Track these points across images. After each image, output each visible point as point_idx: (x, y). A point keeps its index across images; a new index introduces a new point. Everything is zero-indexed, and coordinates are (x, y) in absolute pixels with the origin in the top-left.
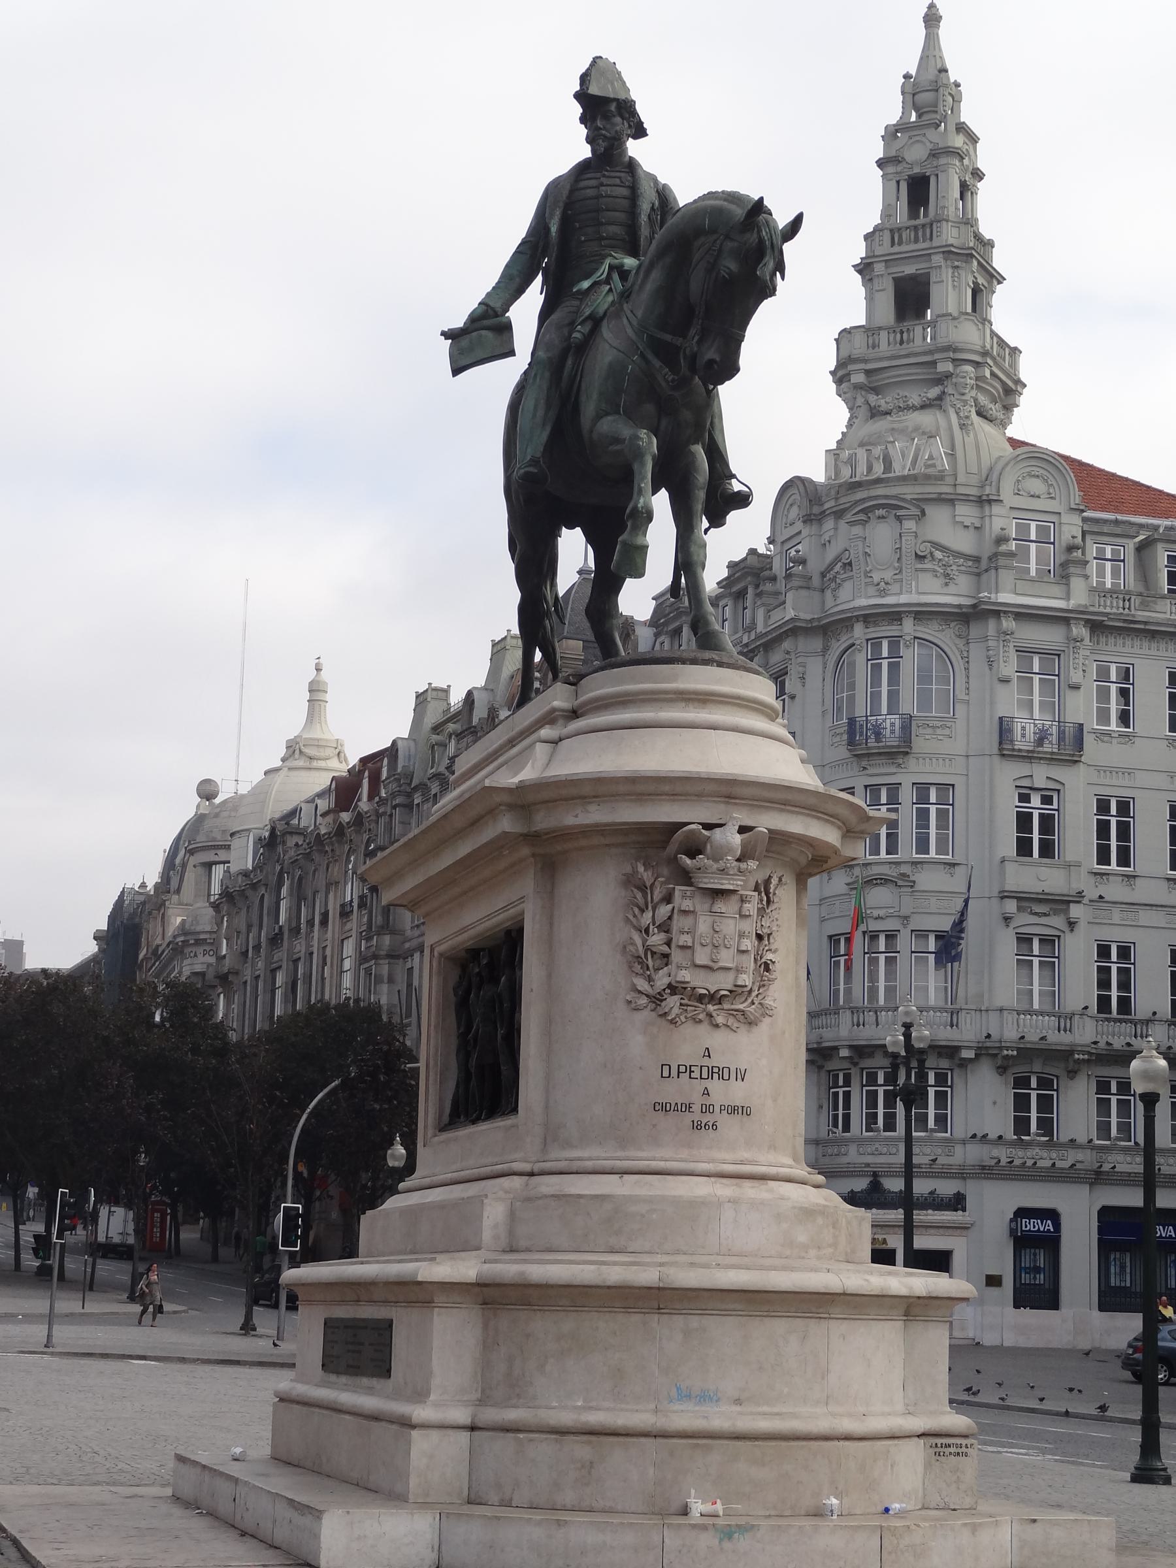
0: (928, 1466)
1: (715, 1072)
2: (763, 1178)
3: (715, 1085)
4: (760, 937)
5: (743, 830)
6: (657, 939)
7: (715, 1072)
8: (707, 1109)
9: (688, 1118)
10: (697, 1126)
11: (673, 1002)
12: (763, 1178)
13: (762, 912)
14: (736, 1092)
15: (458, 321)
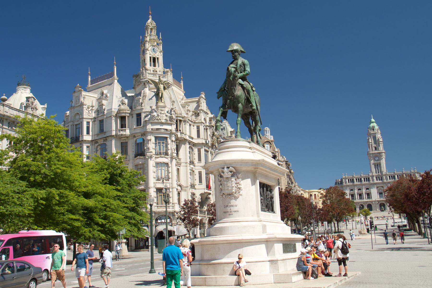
0: (270, 266)
1: (232, 206)
2: (240, 222)
3: (232, 208)
4: (236, 183)
5: (228, 168)
6: (221, 186)
7: (232, 206)
8: (231, 212)
9: (228, 213)
10: (230, 215)
11: (224, 196)
12: (240, 222)
13: (236, 180)
14: (235, 209)
15: (218, 91)
